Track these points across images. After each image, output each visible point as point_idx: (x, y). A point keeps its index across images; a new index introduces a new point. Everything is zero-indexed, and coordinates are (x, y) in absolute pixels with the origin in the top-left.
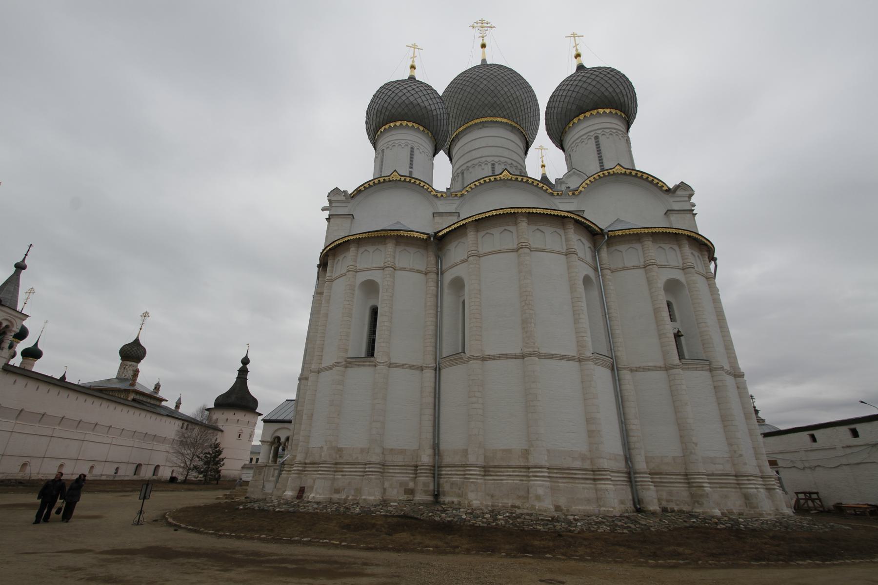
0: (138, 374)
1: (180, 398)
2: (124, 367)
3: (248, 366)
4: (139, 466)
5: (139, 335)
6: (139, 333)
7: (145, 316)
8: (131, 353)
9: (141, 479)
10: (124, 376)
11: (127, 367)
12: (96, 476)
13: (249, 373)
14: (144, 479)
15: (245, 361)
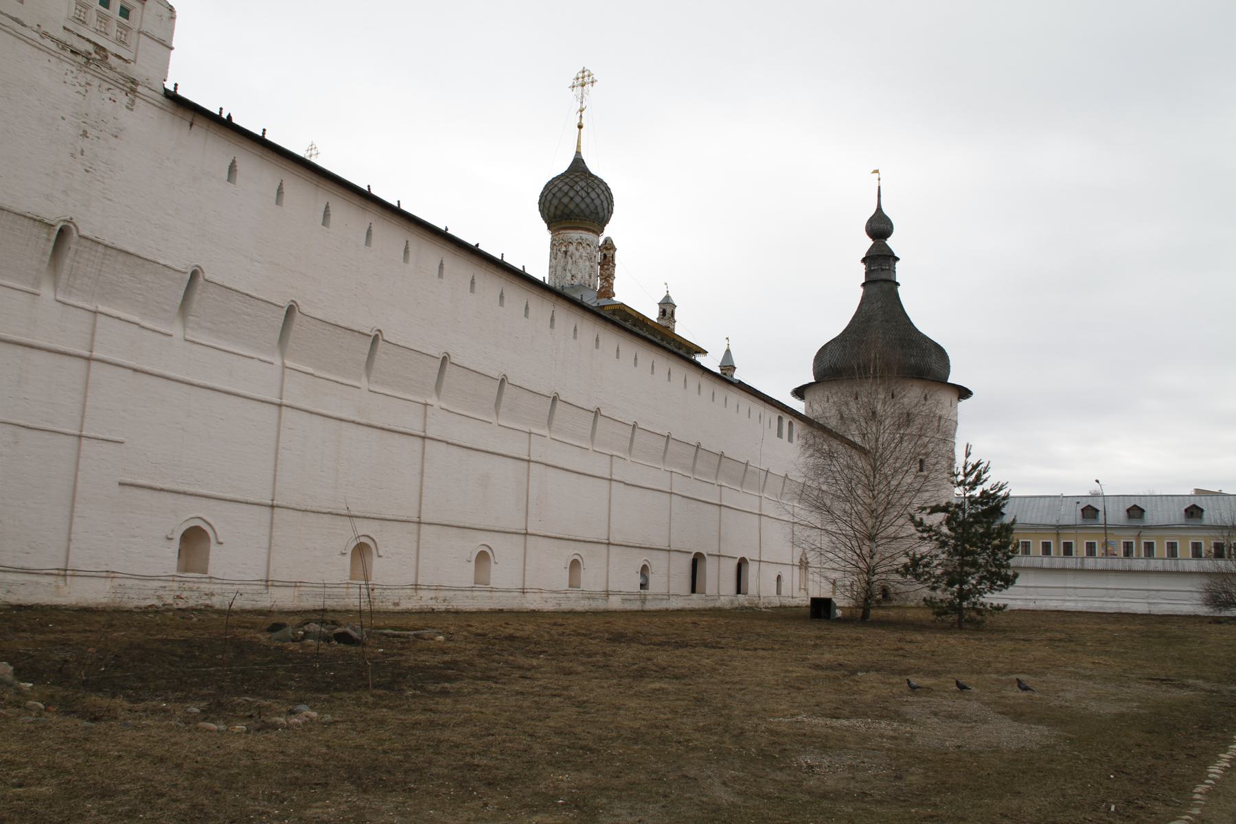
0: (613, 257)
1: (728, 351)
2: (564, 249)
3: (890, 242)
4: (697, 561)
5: (579, 146)
6: (579, 141)
7: (583, 85)
8: (572, 199)
9: (710, 605)
10: (569, 277)
11: (571, 248)
12: (591, 597)
13: (898, 264)
14: (718, 604)
15: (879, 228)
